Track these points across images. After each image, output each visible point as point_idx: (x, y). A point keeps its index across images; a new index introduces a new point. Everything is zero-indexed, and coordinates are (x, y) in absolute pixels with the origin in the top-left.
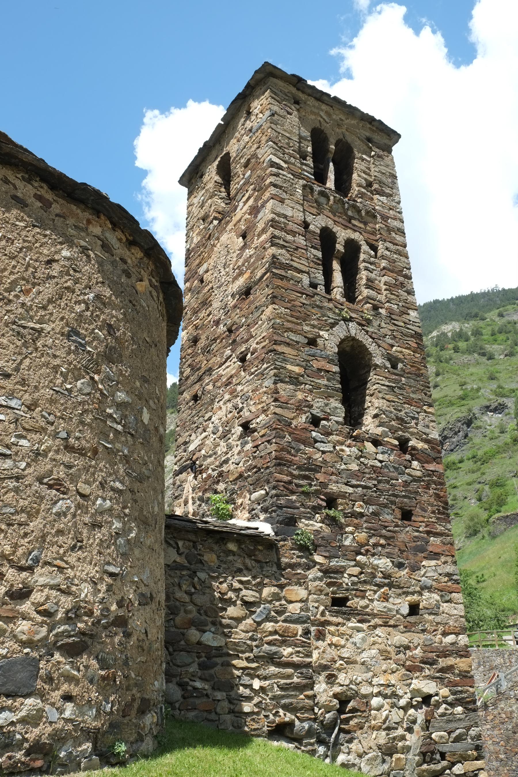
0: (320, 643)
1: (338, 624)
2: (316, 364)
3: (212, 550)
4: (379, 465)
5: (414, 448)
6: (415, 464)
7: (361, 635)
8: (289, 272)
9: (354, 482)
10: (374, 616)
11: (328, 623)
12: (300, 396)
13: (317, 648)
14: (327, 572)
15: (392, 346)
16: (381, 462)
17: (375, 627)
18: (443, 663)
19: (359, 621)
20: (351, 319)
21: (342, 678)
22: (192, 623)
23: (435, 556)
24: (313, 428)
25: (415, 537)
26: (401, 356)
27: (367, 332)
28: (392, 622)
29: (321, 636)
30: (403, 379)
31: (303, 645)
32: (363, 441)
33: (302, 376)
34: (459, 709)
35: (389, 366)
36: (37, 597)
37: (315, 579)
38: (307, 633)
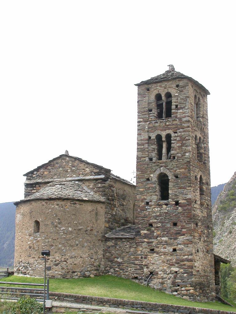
0: (146, 260)
1: (150, 255)
3: (120, 241)
4: (167, 211)
5: (180, 203)
7: (157, 257)
9: (158, 218)
10: (161, 252)
11: (148, 255)
12: (143, 198)
13: (144, 261)
14: (148, 243)
15: (176, 170)
17: (161, 255)
18: (182, 263)
19: (156, 254)
20: (162, 166)
21: (151, 268)
22: (115, 257)
23: (184, 235)
26: (179, 173)
27: (167, 169)
28: (166, 254)
29: (145, 258)
30: (179, 181)
33: (144, 191)
34: (186, 275)
35: (174, 178)
36: (50, 259)
37: (145, 245)
38: (142, 258)
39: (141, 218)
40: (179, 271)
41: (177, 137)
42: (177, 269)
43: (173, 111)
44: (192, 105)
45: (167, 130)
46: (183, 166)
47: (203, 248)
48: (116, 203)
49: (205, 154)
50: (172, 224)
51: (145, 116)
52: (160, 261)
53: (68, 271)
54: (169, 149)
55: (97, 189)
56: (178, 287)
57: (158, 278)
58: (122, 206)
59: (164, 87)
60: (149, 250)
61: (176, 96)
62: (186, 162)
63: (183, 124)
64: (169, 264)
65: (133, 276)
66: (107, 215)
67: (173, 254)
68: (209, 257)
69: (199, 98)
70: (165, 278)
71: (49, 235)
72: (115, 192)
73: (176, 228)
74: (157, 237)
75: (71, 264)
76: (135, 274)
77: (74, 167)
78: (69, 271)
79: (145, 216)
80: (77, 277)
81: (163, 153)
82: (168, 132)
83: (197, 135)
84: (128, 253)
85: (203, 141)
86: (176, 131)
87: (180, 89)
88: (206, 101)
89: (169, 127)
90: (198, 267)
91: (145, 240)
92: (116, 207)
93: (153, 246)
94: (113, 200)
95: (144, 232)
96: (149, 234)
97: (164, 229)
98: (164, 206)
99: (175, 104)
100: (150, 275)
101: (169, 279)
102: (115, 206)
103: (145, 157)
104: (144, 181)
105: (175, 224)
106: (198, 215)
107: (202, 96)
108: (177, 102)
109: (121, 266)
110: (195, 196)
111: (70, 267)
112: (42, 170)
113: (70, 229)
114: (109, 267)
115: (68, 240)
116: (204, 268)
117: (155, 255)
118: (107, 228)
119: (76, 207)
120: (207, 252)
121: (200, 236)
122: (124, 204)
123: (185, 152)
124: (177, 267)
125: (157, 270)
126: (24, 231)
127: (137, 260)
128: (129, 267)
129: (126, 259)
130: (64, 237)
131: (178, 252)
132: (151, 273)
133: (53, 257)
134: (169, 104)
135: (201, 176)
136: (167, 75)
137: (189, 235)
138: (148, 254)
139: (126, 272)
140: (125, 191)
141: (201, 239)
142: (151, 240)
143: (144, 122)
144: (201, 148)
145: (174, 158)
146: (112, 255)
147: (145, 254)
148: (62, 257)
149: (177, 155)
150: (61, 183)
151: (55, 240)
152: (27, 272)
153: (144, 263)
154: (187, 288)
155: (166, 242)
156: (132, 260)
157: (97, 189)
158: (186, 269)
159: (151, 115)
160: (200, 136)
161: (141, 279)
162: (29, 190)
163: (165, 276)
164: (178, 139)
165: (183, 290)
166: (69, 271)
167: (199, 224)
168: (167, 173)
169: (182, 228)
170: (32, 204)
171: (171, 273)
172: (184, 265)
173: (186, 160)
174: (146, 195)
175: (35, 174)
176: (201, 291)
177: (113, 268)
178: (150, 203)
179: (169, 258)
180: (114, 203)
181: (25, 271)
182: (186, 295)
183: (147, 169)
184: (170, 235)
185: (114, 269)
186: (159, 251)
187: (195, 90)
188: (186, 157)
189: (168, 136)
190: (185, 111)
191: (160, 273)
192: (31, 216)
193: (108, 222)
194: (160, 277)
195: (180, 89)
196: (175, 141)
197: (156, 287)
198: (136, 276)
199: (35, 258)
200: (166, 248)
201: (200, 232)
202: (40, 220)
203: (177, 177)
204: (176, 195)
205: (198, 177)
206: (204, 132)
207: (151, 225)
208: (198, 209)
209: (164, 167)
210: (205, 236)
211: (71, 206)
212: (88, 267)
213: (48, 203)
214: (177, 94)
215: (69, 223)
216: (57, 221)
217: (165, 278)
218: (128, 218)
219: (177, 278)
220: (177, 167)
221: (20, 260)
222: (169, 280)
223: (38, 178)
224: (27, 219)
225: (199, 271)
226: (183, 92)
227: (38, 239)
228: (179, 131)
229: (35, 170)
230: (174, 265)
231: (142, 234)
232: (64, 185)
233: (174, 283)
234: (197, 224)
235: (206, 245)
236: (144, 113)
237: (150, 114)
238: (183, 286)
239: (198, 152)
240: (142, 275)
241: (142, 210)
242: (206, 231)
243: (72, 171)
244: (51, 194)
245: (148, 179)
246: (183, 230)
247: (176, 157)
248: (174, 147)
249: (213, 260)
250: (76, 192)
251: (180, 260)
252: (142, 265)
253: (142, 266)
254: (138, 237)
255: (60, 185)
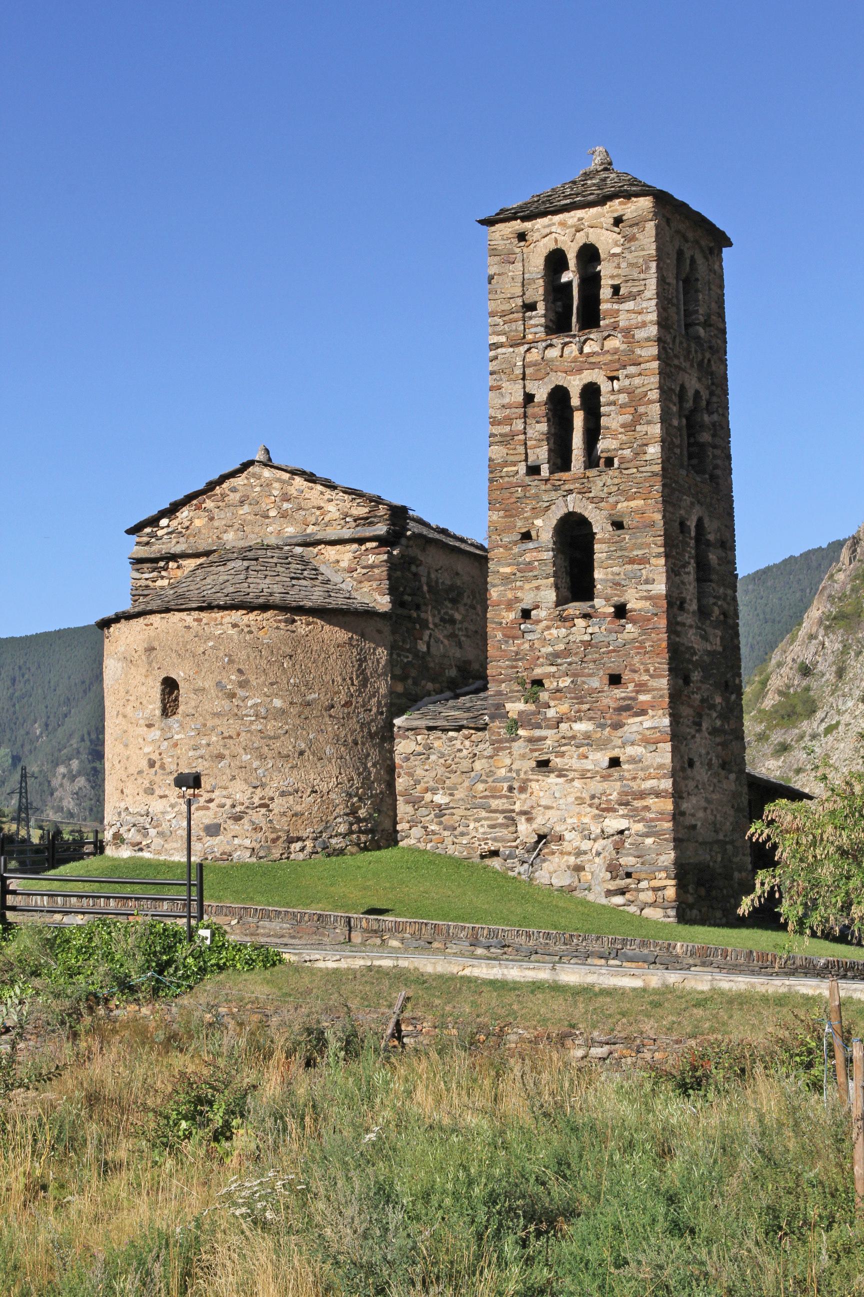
0: (523, 796)
2: (528, 557)
4: (587, 638)
6: (629, 627)
8: (505, 469)
11: (531, 780)
12: (510, 595)
13: (519, 799)
16: (591, 634)
17: (573, 780)
19: (559, 776)
20: (570, 492)
21: (539, 820)
22: (427, 790)
23: (643, 712)
24: (522, 621)
25: (622, 698)
28: (589, 775)
29: (523, 790)
30: (627, 537)
31: (507, 797)
32: (573, 619)
33: (515, 574)
34: (649, 841)
37: (520, 747)
38: (511, 789)
39: (508, 660)
40: (628, 829)
41: (620, 391)
42: (622, 824)
43: (604, 307)
44: (669, 284)
45: (586, 372)
46: (640, 490)
47: (708, 753)
48: (430, 617)
49: (715, 447)
50: (606, 680)
51: (514, 327)
52: (571, 799)
53: (274, 836)
54: (593, 433)
55: (365, 571)
56: (629, 881)
57: (562, 853)
58: (447, 625)
59: (572, 226)
60: (534, 764)
61: (614, 255)
62: (649, 474)
63: (638, 351)
64: (597, 808)
65: (483, 846)
66: (399, 655)
67: (610, 776)
68: (730, 783)
69: (693, 260)
70: (585, 853)
71: (210, 724)
72: (424, 580)
73: (618, 692)
74: (560, 721)
75: (284, 814)
76: (490, 842)
77: (288, 500)
78: (278, 838)
79: (517, 656)
80: (301, 856)
81: (574, 446)
82: (588, 376)
83: (687, 385)
84: (468, 775)
85: (708, 403)
86: (615, 374)
87: (628, 231)
88: (716, 267)
89: (592, 360)
90: (693, 815)
91: (521, 732)
92: (428, 628)
93: (546, 750)
94: (418, 607)
95: (515, 708)
96: (533, 713)
97: (579, 695)
98: (580, 623)
99: (611, 282)
100: (538, 842)
101: (598, 854)
102: (424, 625)
103: (514, 464)
104: (515, 543)
105: (615, 680)
106: (692, 647)
107: (702, 251)
108: (618, 276)
109: (447, 817)
110: (678, 587)
111: (281, 824)
112: (185, 514)
113: (278, 703)
114: (408, 822)
115: (270, 738)
116: (713, 818)
117: (552, 779)
118: (399, 695)
119: (294, 632)
120: (723, 766)
121: (700, 715)
122: (458, 616)
123: (645, 442)
124: (623, 816)
125: (558, 828)
126: (129, 709)
127: (493, 797)
128: (472, 818)
129: (460, 794)
130: (259, 727)
131: (625, 766)
132: (541, 837)
133: (225, 793)
134: (591, 282)
135: (700, 521)
136: (583, 185)
137: (661, 711)
138: (531, 777)
139: (462, 834)
140: (457, 574)
141: (699, 724)
142: (537, 733)
143: (511, 346)
144: (702, 426)
145: (609, 462)
146: (418, 782)
147: (522, 776)
148: (253, 793)
149: (620, 452)
150: (248, 553)
151: (231, 737)
152: (144, 843)
153: (517, 807)
154: (655, 883)
155: (587, 736)
156: (480, 798)
157: (365, 571)
158: (652, 820)
159: (532, 322)
160: (698, 386)
161: (510, 856)
162: (147, 579)
163: (586, 845)
164: (623, 398)
165: (643, 890)
166: (278, 838)
167: (696, 676)
168: (586, 514)
169: (637, 692)
170: (152, 624)
171: (603, 835)
172: (647, 808)
173: (648, 468)
174: (521, 588)
175: (163, 528)
176: (702, 892)
177: (420, 825)
178: (533, 613)
179: (596, 786)
180: (423, 615)
181: (138, 838)
182: (653, 904)
183: (524, 500)
184: (599, 713)
185: (425, 828)
186: (567, 767)
187: (678, 232)
188: (648, 457)
189: (591, 392)
190: (644, 305)
191: (568, 836)
192: (150, 664)
193: (403, 678)
194: (569, 849)
195: (628, 231)
196: (613, 408)
197: (556, 880)
198: (493, 848)
199: (165, 796)
200: (587, 757)
201: (697, 703)
202: (178, 675)
203: (618, 525)
204: (618, 584)
205: (688, 523)
206: (712, 374)
207: (538, 683)
208: (691, 626)
209: (579, 493)
210: (715, 715)
211: (278, 628)
212: (340, 823)
213: (205, 621)
214: (617, 250)
215: (272, 684)
216: (233, 677)
217: (585, 853)
218: (469, 662)
219: (624, 852)
220: (620, 492)
221: (123, 805)
222: (597, 860)
223: (174, 541)
224: (137, 674)
225: (694, 827)
226: (637, 239)
227: (176, 737)
228: (625, 372)
229: (163, 514)
230: (614, 810)
231: (510, 715)
232: (256, 559)
233: (613, 869)
234: (687, 680)
235: (718, 744)
236: (511, 316)
237: (531, 318)
238: (643, 876)
239: (692, 440)
240: (514, 844)
241: (509, 637)
242: (718, 700)
243: (284, 515)
244: (213, 590)
245: (526, 536)
246: (642, 698)
247: (616, 460)
248: (608, 428)
249: (745, 790)
250: (294, 582)
251: (633, 793)
252: (513, 811)
253: (514, 815)
254: (497, 723)
255: (243, 560)
